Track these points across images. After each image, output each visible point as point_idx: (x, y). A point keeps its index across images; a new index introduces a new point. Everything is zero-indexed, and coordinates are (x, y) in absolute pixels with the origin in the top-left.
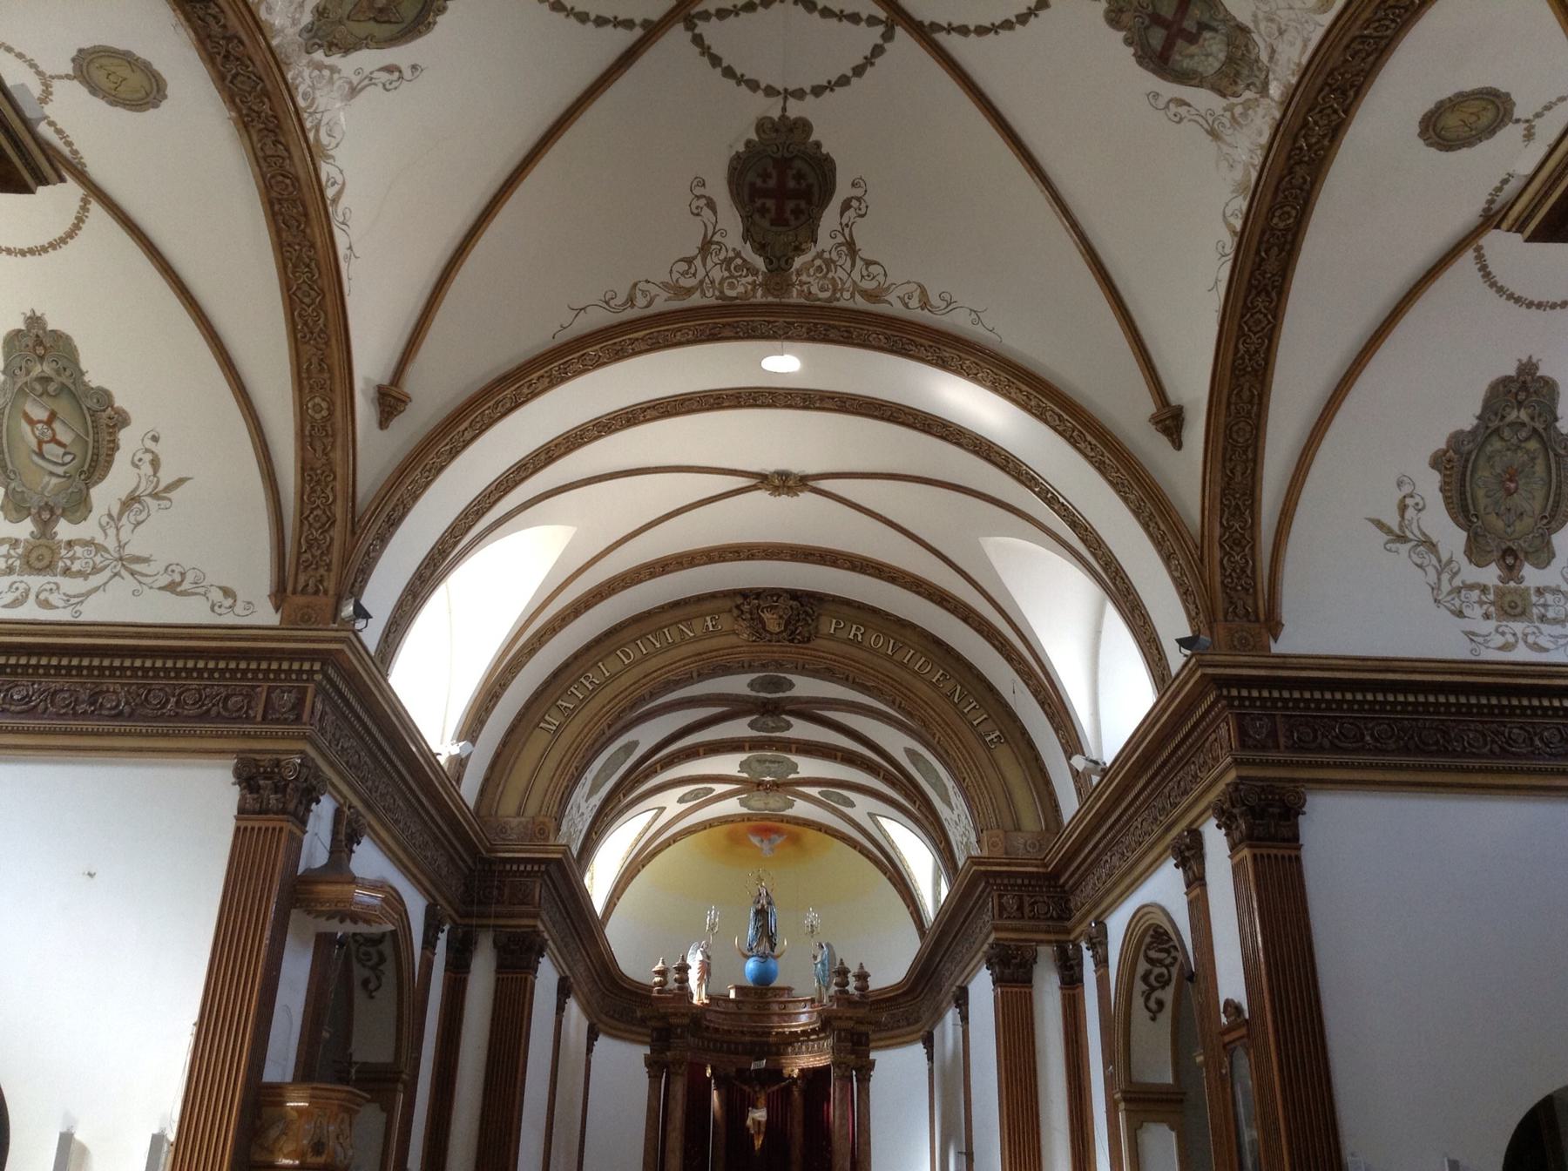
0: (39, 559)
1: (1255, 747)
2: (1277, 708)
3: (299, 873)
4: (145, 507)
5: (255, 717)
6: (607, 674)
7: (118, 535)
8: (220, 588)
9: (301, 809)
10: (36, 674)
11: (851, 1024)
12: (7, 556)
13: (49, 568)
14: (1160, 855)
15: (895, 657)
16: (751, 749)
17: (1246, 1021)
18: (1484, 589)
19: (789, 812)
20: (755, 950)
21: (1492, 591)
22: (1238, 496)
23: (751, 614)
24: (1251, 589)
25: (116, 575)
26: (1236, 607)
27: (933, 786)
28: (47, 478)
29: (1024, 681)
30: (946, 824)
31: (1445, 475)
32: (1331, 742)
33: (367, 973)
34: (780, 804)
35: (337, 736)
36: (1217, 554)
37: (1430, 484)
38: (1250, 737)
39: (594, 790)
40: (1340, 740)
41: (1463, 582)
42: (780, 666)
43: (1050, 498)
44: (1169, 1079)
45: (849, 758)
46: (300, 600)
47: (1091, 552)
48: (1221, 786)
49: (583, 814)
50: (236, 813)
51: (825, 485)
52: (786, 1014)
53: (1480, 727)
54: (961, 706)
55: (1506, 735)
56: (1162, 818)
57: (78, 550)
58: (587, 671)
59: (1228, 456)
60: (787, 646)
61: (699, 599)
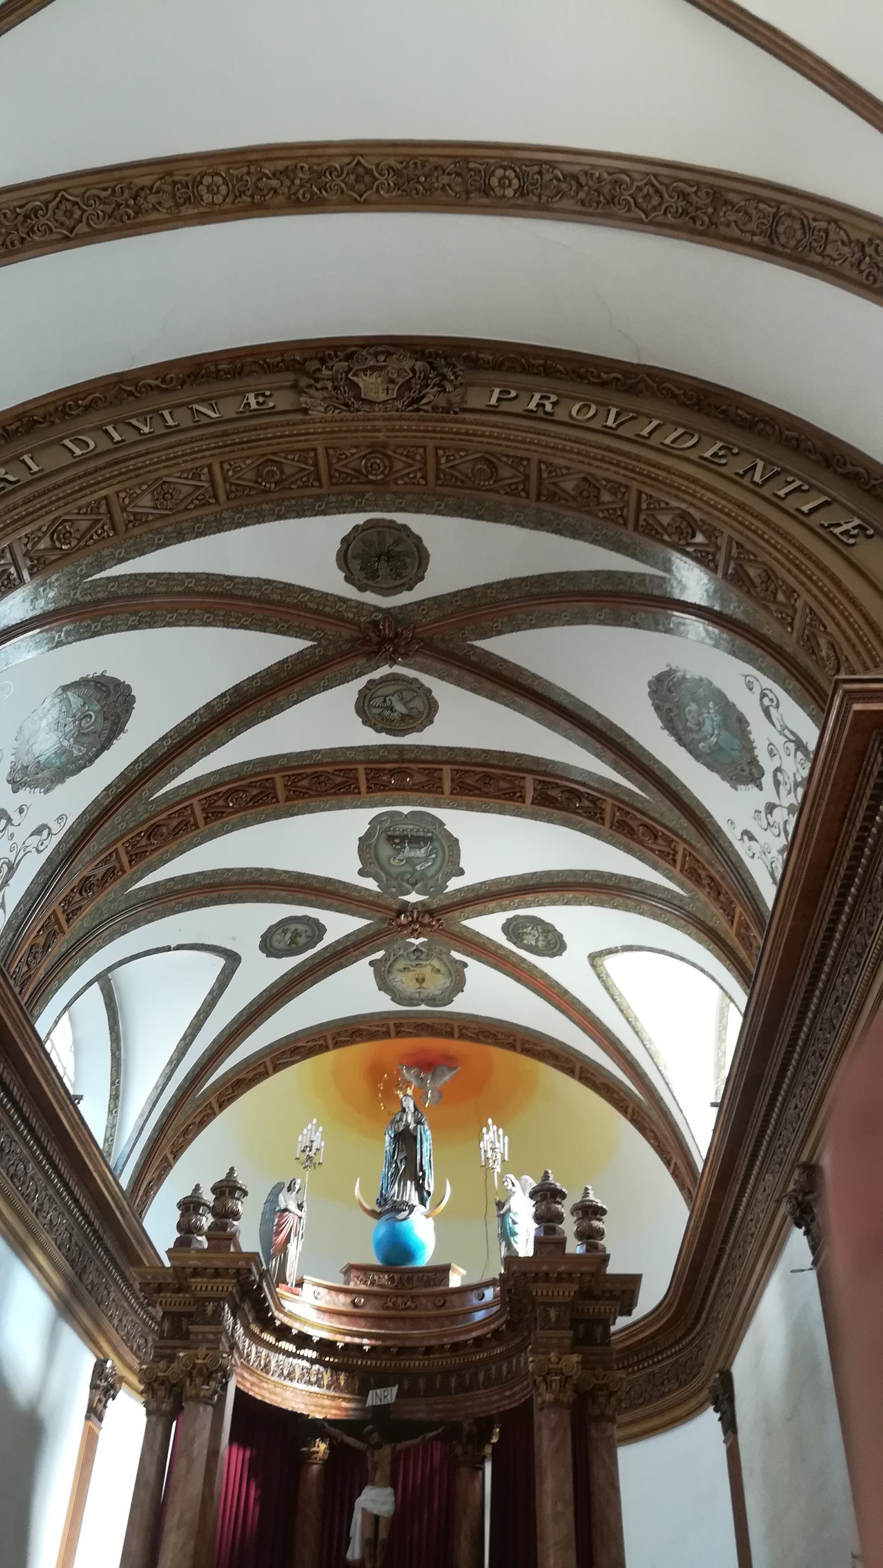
52: (447, 1317)
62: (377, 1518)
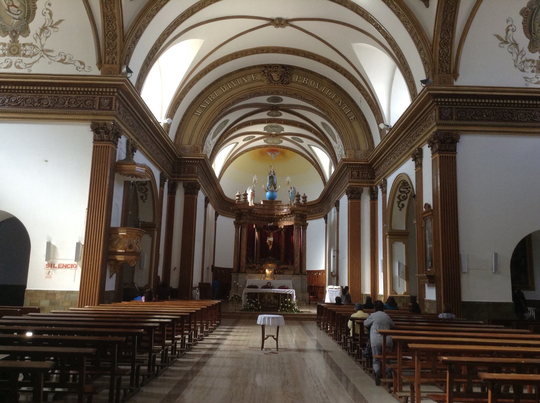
0: (14, 50)
1: (445, 119)
2: (454, 105)
3: (117, 161)
4: (49, 31)
5: (96, 108)
6: (217, 96)
7: (40, 41)
8: (79, 61)
9: (115, 140)
10: (18, 92)
11: (300, 212)
12: (3, 50)
13: (17, 54)
14: (408, 156)
15: (319, 89)
16: (268, 122)
17: (432, 210)
18: (533, 61)
19: (281, 144)
20: (269, 189)
21: (536, 62)
22: (448, 26)
23: (268, 74)
24: (449, 62)
25: (42, 56)
26: (443, 68)
27: (330, 135)
28: (12, 20)
29: (364, 97)
30: (334, 148)
31: (525, 18)
32: (471, 117)
33: (142, 194)
34: (278, 142)
35: (125, 115)
36: (438, 48)
37: (519, 21)
38: (443, 115)
39: (214, 137)
40: (474, 116)
41: (526, 59)
42: (278, 93)
43: (379, 27)
44: (404, 229)
45: (302, 126)
46: (107, 66)
47: (392, 48)
48: (431, 133)
49: (211, 144)
50: (93, 141)
51: (295, 23)
52: (279, 209)
53: (525, 112)
54: (341, 107)
55: (534, 114)
56: (409, 144)
57: (27, 47)
58: (210, 95)
59: (445, 10)
60: (280, 86)
61: (249, 68)
62: (271, 241)
